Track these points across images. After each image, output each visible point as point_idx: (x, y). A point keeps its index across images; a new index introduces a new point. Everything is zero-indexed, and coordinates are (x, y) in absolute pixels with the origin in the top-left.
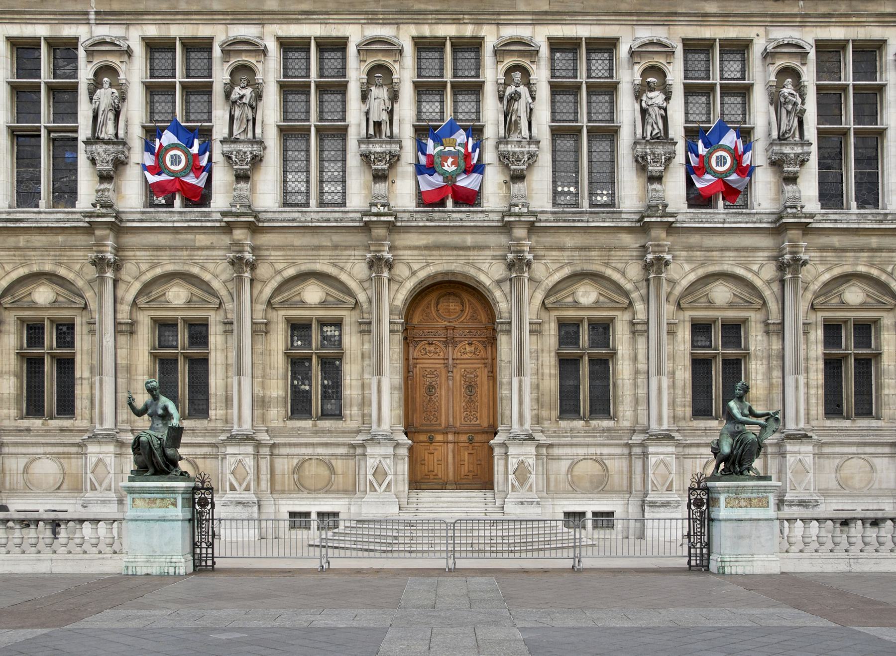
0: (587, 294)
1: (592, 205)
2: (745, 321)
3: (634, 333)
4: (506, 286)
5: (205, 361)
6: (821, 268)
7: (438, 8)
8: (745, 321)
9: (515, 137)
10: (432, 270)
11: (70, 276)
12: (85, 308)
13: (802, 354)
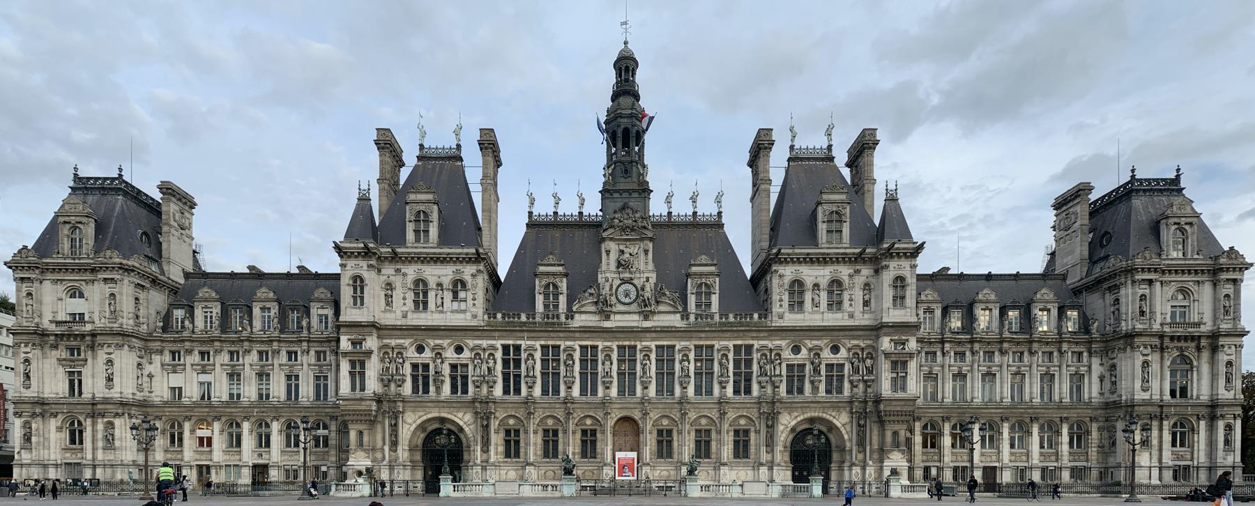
0: (665, 422)
1: (667, 395)
2: (711, 429)
3: (678, 433)
4: (642, 420)
5: (557, 441)
8: (711, 429)
9: (645, 377)
10: (621, 415)
11: (519, 416)
12: (524, 425)
13: (726, 440)
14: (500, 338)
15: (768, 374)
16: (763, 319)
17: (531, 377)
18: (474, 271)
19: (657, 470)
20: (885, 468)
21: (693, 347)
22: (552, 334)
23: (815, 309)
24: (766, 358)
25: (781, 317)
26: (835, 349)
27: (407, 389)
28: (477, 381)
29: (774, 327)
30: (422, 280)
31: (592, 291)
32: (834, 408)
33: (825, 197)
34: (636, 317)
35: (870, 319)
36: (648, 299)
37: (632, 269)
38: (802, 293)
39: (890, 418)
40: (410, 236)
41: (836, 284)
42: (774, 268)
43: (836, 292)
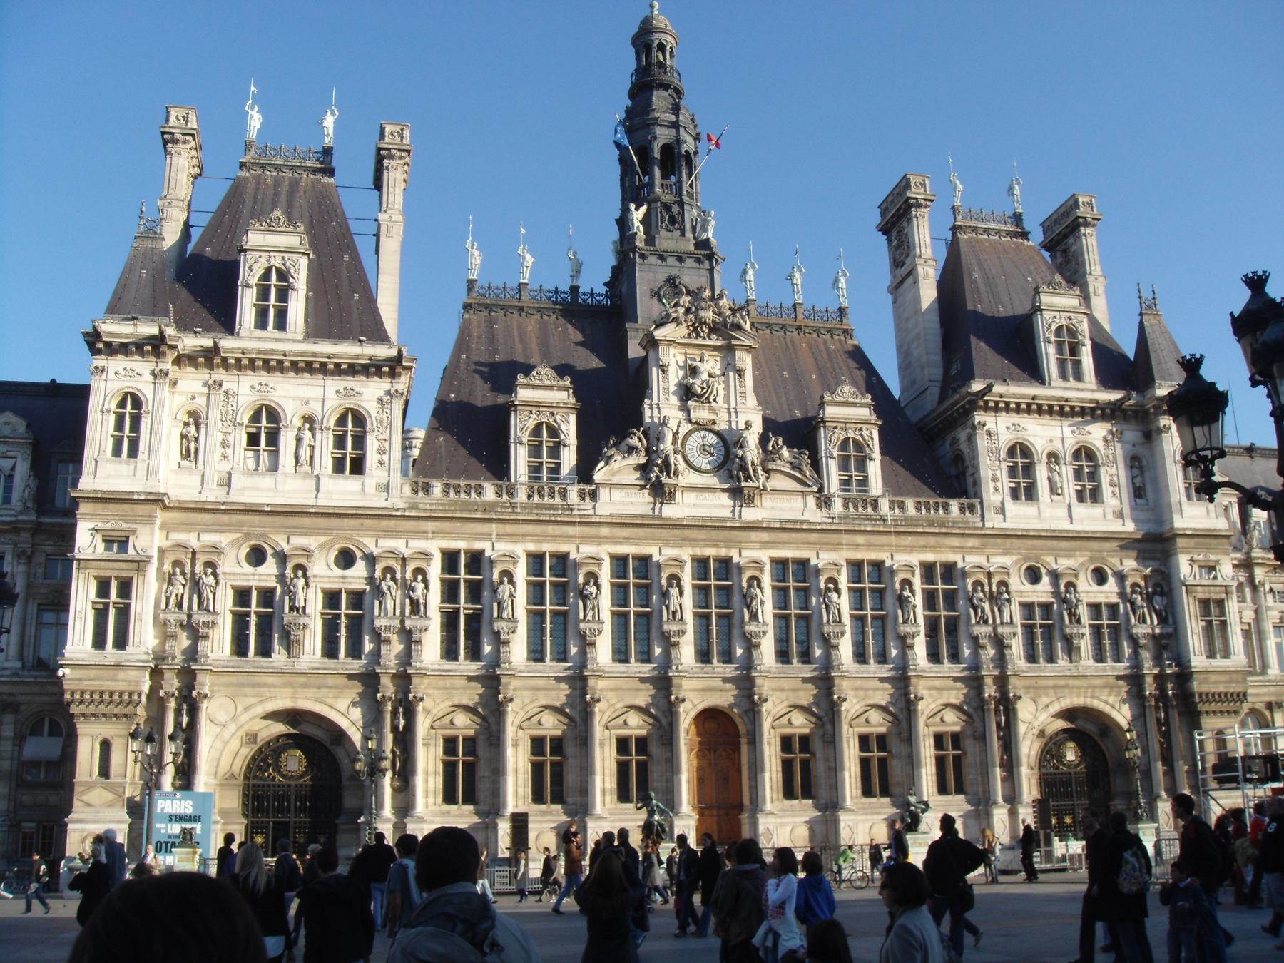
4: (751, 714)
7: (704, 537)
14: (436, 534)
15: (990, 621)
16: (967, 513)
17: (509, 620)
19: (783, 825)
21: (844, 563)
22: (550, 529)
23: (1055, 497)
24: (983, 591)
25: (1002, 511)
26: (1100, 577)
27: (219, 645)
28: (388, 629)
30: (266, 405)
31: (634, 441)
34: (725, 499)
35: (1148, 521)
36: (753, 464)
37: (714, 404)
38: (1029, 469)
39: (1206, 707)
41: (1085, 453)
42: (979, 417)
43: (1086, 470)
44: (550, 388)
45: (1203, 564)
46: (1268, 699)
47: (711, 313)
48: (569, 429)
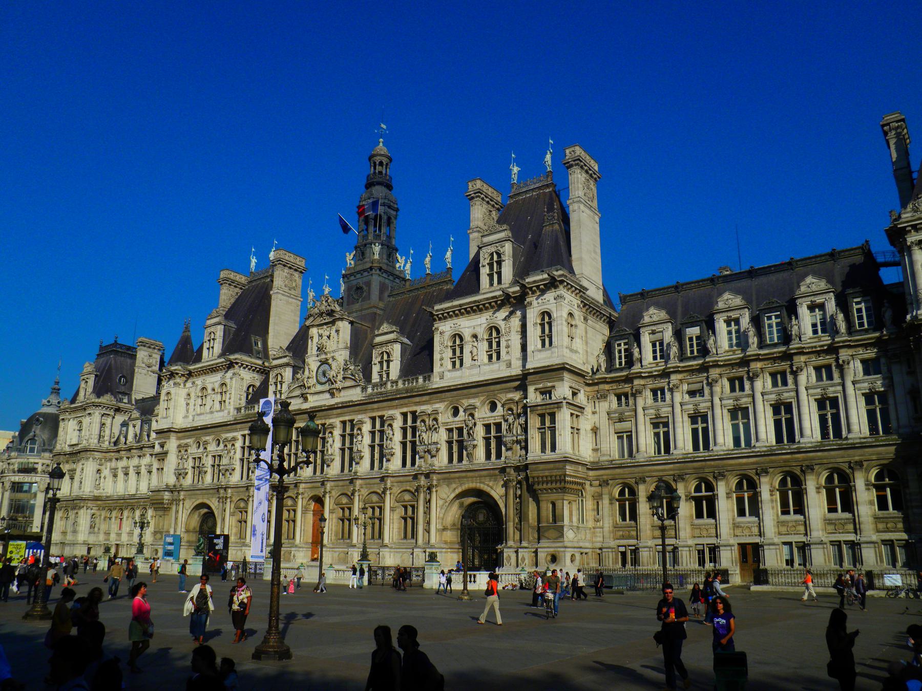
6: (398, 488)
10: (312, 494)
15: (426, 442)
18: (232, 374)
19: (335, 552)
20: (539, 550)
25: (442, 378)
26: (493, 407)
29: (430, 389)
32: (490, 476)
33: (486, 240)
34: (327, 395)
36: (333, 377)
40: (205, 353)
41: (494, 329)
42: (436, 326)
44: (281, 358)
45: (543, 390)
46: (671, 472)
47: (323, 307)
48: (288, 373)
